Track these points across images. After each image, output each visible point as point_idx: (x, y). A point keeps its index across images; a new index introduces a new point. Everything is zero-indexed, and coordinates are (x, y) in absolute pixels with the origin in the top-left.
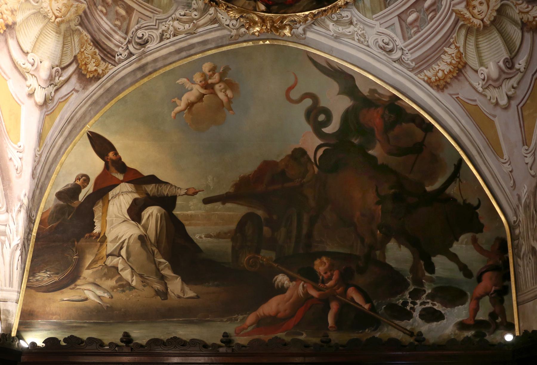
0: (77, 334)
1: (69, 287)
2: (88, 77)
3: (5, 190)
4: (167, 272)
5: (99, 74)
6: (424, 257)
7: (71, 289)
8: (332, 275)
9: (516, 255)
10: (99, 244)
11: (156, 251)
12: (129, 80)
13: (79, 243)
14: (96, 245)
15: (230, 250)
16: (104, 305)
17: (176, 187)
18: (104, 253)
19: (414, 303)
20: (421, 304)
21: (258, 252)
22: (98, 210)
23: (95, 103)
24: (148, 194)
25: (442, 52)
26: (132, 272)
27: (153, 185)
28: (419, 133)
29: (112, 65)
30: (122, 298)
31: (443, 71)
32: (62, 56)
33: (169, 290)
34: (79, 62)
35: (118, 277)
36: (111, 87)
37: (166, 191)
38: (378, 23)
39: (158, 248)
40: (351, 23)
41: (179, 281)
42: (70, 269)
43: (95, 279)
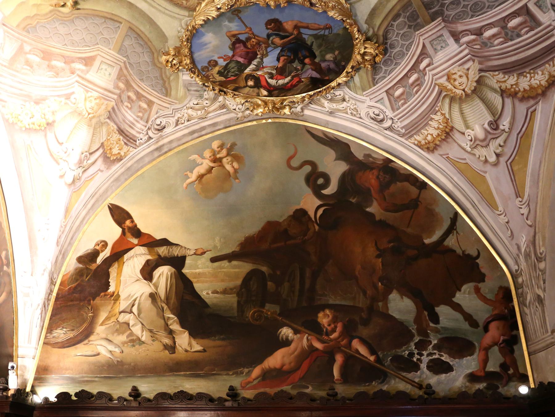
0: (87, 388)
1: (83, 343)
3: (32, 257)
4: (176, 327)
6: (427, 308)
7: (84, 344)
8: (336, 327)
9: (522, 304)
10: (113, 302)
11: (165, 307)
13: (95, 302)
14: (110, 303)
15: (235, 305)
16: (115, 360)
17: (185, 248)
18: (117, 311)
19: (421, 355)
20: (428, 355)
21: (263, 306)
22: (113, 271)
24: (159, 256)
26: (142, 327)
27: (165, 247)
28: (414, 191)
30: (133, 354)
31: (432, 135)
33: (177, 344)
35: (129, 332)
37: (176, 252)
39: (167, 304)
41: (186, 334)
42: (85, 325)
43: (107, 335)
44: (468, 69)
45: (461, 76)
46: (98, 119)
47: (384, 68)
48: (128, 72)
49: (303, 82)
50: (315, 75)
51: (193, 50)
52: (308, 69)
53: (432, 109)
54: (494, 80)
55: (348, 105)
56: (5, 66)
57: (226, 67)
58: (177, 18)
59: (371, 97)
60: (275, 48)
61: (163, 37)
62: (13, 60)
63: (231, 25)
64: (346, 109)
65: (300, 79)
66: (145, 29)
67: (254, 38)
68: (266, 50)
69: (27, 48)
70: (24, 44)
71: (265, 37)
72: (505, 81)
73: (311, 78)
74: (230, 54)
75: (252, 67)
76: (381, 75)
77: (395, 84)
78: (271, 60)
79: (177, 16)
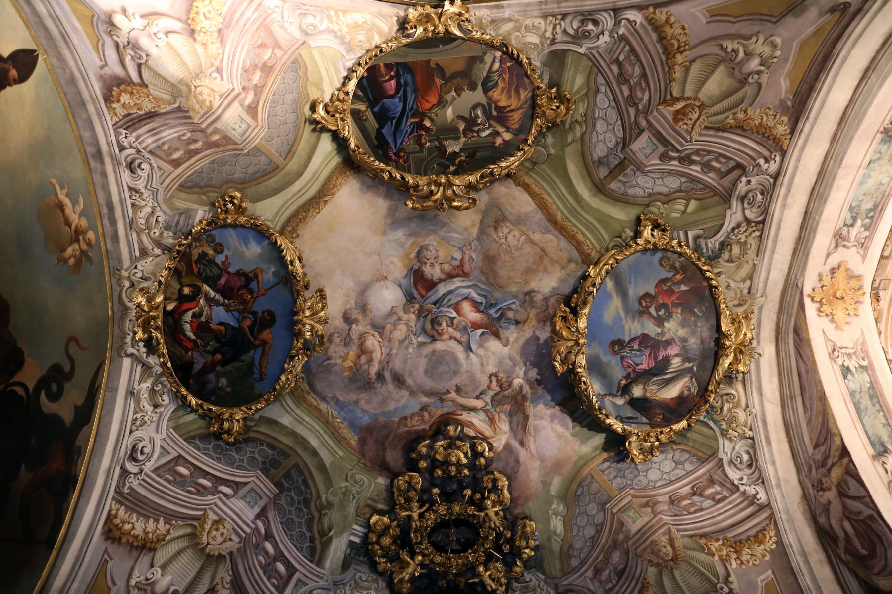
2: (115, 89)
5: (113, 102)
12: (86, 135)
25: (156, 517)
29: (117, 123)
31: (133, 528)
32: (155, 72)
36: (86, 110)
44: (231, 540)
45: (222, 534)
47: (210, 447)
48: (229, 151)
50: (197, 368)
52: (205, 358)
53: (170, 516)
54: (224, 574)
55: (149, 413)
56: (265, 20)
57: (212, 262)
59: (168, 440)
60: (238, 320)
62: (270, 32)
63: (270, 274)
64: (142, 411)
65: (191, 350)
66: (272, 182)
69: (278, 53)
70: (282, 53)
71: (255, 309)
72: (223, 586)
73: (193, 363)
75: (212, 293)
76: (201, 445)
77: (192, 464)
78: (220, 314)
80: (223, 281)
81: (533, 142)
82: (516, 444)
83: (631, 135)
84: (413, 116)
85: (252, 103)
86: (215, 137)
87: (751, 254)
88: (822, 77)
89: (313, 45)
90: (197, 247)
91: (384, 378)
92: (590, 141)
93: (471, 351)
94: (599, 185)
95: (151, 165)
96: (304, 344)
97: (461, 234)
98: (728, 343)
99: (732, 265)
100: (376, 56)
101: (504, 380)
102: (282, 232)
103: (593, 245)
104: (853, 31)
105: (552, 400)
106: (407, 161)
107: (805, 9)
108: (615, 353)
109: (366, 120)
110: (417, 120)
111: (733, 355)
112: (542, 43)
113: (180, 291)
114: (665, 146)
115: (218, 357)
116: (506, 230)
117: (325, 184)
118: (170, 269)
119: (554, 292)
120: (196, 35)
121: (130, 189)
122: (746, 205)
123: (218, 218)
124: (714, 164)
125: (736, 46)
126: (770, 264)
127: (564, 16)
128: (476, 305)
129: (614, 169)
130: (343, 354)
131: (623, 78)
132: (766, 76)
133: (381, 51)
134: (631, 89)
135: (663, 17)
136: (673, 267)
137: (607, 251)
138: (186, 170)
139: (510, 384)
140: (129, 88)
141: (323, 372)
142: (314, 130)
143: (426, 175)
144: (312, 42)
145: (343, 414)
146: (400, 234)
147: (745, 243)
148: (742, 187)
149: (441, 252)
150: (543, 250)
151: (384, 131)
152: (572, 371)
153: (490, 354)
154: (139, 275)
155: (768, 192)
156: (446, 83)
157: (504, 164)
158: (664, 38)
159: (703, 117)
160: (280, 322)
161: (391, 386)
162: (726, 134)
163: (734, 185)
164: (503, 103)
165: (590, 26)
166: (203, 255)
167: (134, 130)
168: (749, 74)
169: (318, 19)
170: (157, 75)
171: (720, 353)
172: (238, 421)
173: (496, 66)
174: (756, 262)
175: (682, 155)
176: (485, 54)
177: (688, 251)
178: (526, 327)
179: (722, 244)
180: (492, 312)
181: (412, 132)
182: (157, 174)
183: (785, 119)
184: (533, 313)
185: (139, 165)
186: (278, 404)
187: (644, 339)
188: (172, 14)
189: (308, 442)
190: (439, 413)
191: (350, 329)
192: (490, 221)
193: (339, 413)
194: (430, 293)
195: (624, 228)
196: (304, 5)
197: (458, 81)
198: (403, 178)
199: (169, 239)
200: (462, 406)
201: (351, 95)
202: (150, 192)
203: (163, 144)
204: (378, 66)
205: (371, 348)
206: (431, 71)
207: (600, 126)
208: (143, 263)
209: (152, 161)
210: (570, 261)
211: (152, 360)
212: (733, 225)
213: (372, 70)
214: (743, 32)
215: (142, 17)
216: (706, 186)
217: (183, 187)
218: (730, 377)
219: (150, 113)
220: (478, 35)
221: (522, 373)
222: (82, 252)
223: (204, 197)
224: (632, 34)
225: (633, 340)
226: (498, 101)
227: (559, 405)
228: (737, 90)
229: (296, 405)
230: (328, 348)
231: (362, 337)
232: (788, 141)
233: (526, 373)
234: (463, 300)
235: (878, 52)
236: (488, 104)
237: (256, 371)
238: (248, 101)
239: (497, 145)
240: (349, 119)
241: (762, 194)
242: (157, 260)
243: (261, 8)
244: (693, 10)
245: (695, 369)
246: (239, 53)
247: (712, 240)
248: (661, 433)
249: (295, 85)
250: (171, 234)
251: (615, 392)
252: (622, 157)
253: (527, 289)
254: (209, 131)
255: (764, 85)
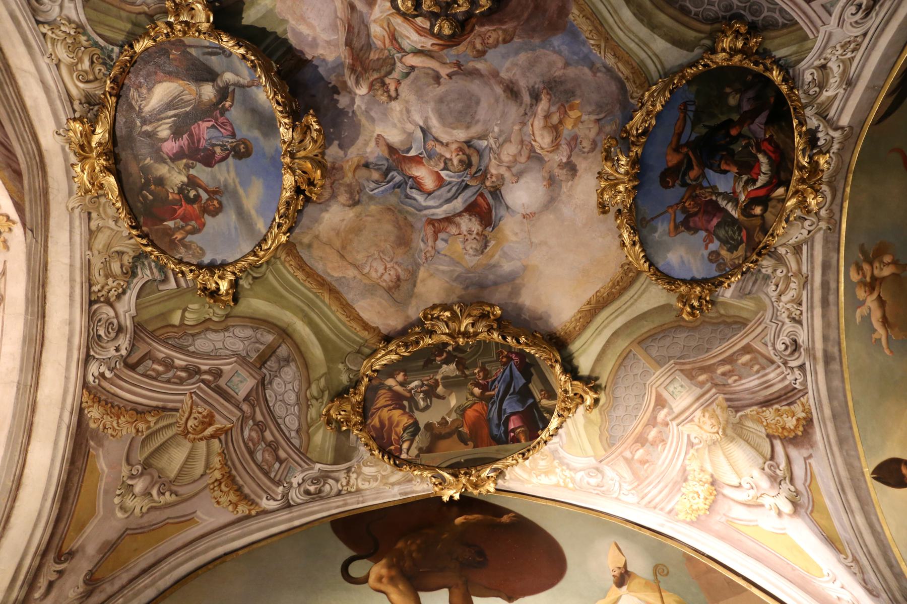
2: (800, 433)
5: (804, 418)
23: (841, 441)
29: (803, 396)
34: (776, 434)
38: (822, 30)
40: (823, 67)
46: (731, 425)
47: (766, 13)
48: (689, 363)
49: (771, 136)
50: (762, 118)
51: (688, 277)
52: (750, 129)
57: (724, 242)
58: (647, 287)
61: (663, 309)
62: (635, 473)
65: (766, 140)
66: (646, 327)
67: (685, 203)
68: (707, 188)
69: (628, 454)
70: (624, 454)
71: (684, 189)
73: (766, 124)
74: (703, 234)
75: (729, 208)
78: (723, 184)
79: (644, 286)
80: (715, 221)
81: (363, 378)
82: (360, 6)
83: (257, 393)
84: (492, 397)
85: (660, 410)
86: (702, 378)
87: (97, 264)
88: (64, 476)
89: (592, 459)
90: (738, 258)
91: (530, 94)
92: (300, 381)
93: (421, 128)
94: (285, 336)
95: (774, 349)
96: (630, 150)
97: (438, 270)
98: (102, 161)
99: (118, 249)
100: (529, 451)
101: (380, 92)
102: (639, 273)
103: (285, 267)
104: (45, 530)
105: (317, 67)
106: (499, 354)
107: (100, 550)
108: (244, 141)
109: (542, 391)
110: (487, 393)
111: (93, 145)
112: (359, 467)
113: (765, 211)
114: (218, 387)
115: (734, 132)
116: (386, 277)
117: (588, 323)
118: (772, 235)
119: (324, 205)
120: (710, 480)
121: (800, 322)
122: (115, 321)
123: (710, 290)
124: (160, 368)
125: (162, 499)
126: (72, 250)
127: (339, 493)
128: (418, 185)
129: (270, 356)
130: (580, 126)
131: (273, 447)
132: (123, 474)
133: (523, 454)
134: (264, 439)
135: (240, 508)
136: (187, 247)
137: (268, 262)
138: (738, 341)
139: (371, 87)
140: (786, 434)
141: (607, 104)
142: (597, 379)
143: (479, 342)
144: (593, 462)
145: (585, 50)
146: (507, 267)
147: (107, 277)
148: (124, 343)
149: (459, 248)
150: (342, 257)
151: (524, 381)
152: (295, 116)
153: (399, 125)
154: (807, 223)
155: (92, 341)
156: (457, 428)
157: (394, 357)
158: (236, 491)
159: (183, 422)
160: (655, 175)
161: (523, 83)
162: (154, 403)
163: (134, 345)
164: (397, 413)
165: (312, 488)
166: (731, 250)
167: (786, 387)
168: (142, 474)
169: (585, 481)
170: (756, 448)
171: (110, 146)
172: (724, 50)
173: (405, 446)
174: (89, 252)
175: (198, 376)
176: (418, 456)
177: (173, 266)
178: (356, 160)
179: (134, 274)
180: (398, 178)
181: (494, 381)
182: (769, 339)
183: (92, 425)
184: (349, 178)
185: (786, 349)
186: (668, 66)
187: (209, 160)
188: (732, 503)
189: (635, 14)
190: (461, 48)
191: (569, 157)
192: (405, 287)
193: (591, 51)
194: (473, 199)
195: (251, 289)
196: (598, 494)
197: (444, 431)
198: (504, 338)
199: (767, 264)
200: (432, 57)
201: (556, 413)
202: (779, 318)
203: (758, 372)
204: (526, 440)
205: (546, 134)
206: (474, 437)
207: (292, 398)
208: (801, 237)
209: (772, 352)
210: (310, 246)
211: (813, 122)
212: (126, 297)
213: (533, 435)
214: (158, 513)
215: (762, 506)
216: (164, 342)
217: (743, 323)
218: (89, 104)
219: (767, 406)
220: (425, 473)
221: (358, 101)
222: (871, 264)
223: (722, 312)
224: (269, 488)
225: (223, 159)
226: (402, 414)
227: (307, 62)
228: (152, 455)
229: (645, 65)
230: (598, 134)
231: (555, 146)
232: (84, 400)
233: (353, 101)
234: (434, 191)
235: (12, 508)
236: (413, 412)
237: (691, 114)
238: (665, 411)
239: (402, 374)
240: (559, 391)
241: (99, 336)
242: (784, 241)
243: (641, 495)
244: (212, 520)
245: (139, 124)
246: (668, 458)
247: (146, 279)
248: (167, 35)
249: (613, 424)
250: (763, 271)
251: (237, 90)
252: (264, 370)
253: (358, 209)
254: (709, 385)
255: (124, 463)
